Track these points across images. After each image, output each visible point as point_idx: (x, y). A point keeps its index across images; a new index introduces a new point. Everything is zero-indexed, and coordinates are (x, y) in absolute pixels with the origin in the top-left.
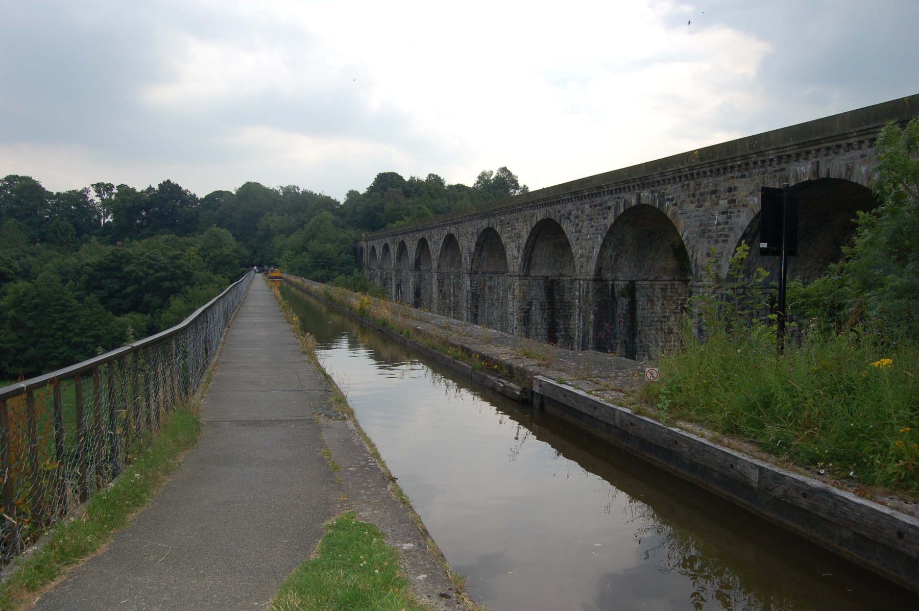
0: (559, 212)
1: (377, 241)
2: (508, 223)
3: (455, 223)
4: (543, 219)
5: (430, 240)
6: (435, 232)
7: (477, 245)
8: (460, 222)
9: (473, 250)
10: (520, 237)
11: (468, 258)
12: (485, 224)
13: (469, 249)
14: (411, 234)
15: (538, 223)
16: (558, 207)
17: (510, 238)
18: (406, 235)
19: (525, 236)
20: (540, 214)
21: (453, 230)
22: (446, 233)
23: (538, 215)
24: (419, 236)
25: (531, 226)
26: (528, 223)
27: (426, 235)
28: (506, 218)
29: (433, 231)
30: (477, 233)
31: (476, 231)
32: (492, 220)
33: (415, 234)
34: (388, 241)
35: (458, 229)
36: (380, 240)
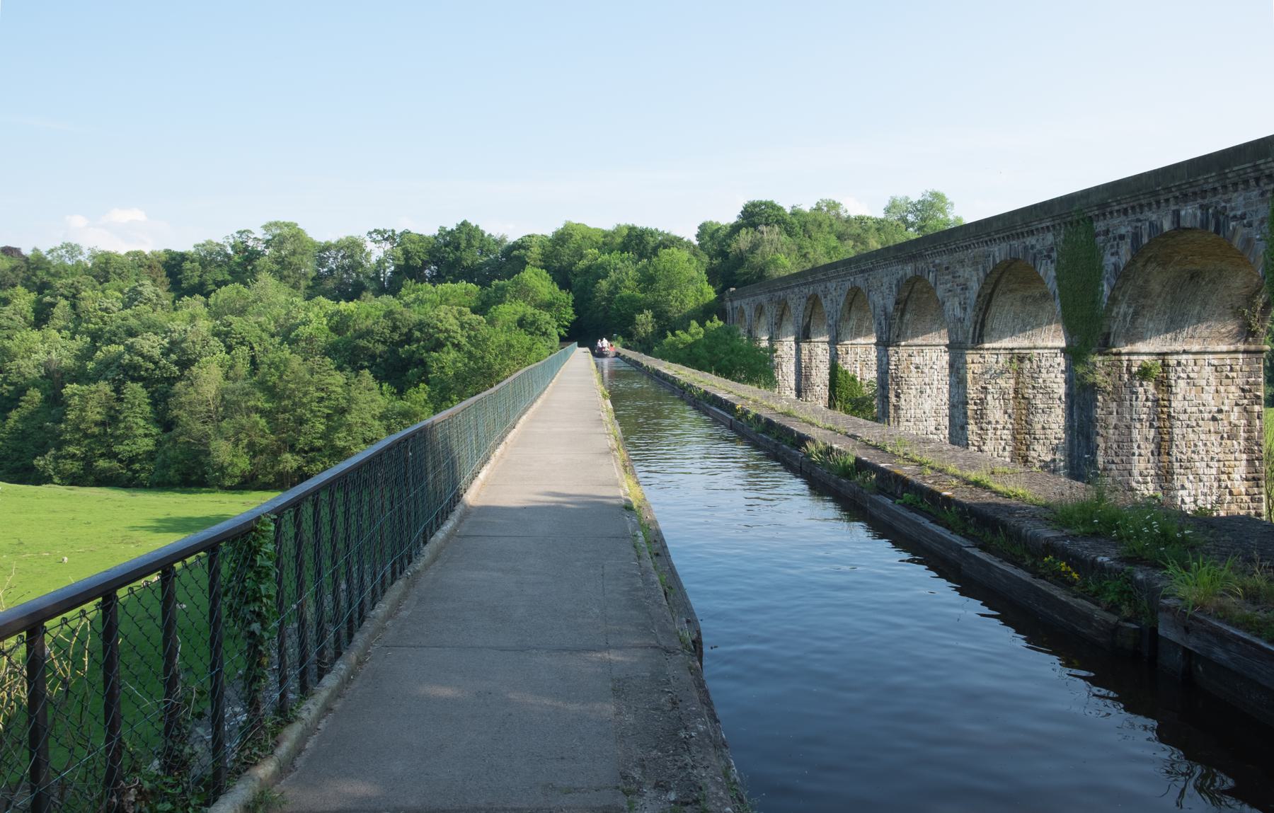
0: (1033, 247)
1: (747, 301)
2: (947, 268)
3: (862, 272)
4: (1006, 261)
5: (825, 297)
6: (832, 285)
7: (897, 303)
8: (871, 270)
9: (891, 309)
10: (966, 289)
11: (883, 322)
12: (909, 269)
13: (885, 309)
14: (796, 290)
15: (996, 267)
16: (1030, 241)
17: (950, 291)
18: (789, 291)
19: (975, 287)
20: (999, 252)
21: (859, 281)
22: (848, 285)
23: (997, 254)
24: (807, 291)
25: (984, 270)
26: (980, 266)
27: (820, 289)
28: (944, 260)
29: (828, 284)
30: (897, 285)
31: (895, 282)
32: (921, 264)
33: (802, 288)
34: (763, 299)
35: (867, 279)
36: (751, 299)
